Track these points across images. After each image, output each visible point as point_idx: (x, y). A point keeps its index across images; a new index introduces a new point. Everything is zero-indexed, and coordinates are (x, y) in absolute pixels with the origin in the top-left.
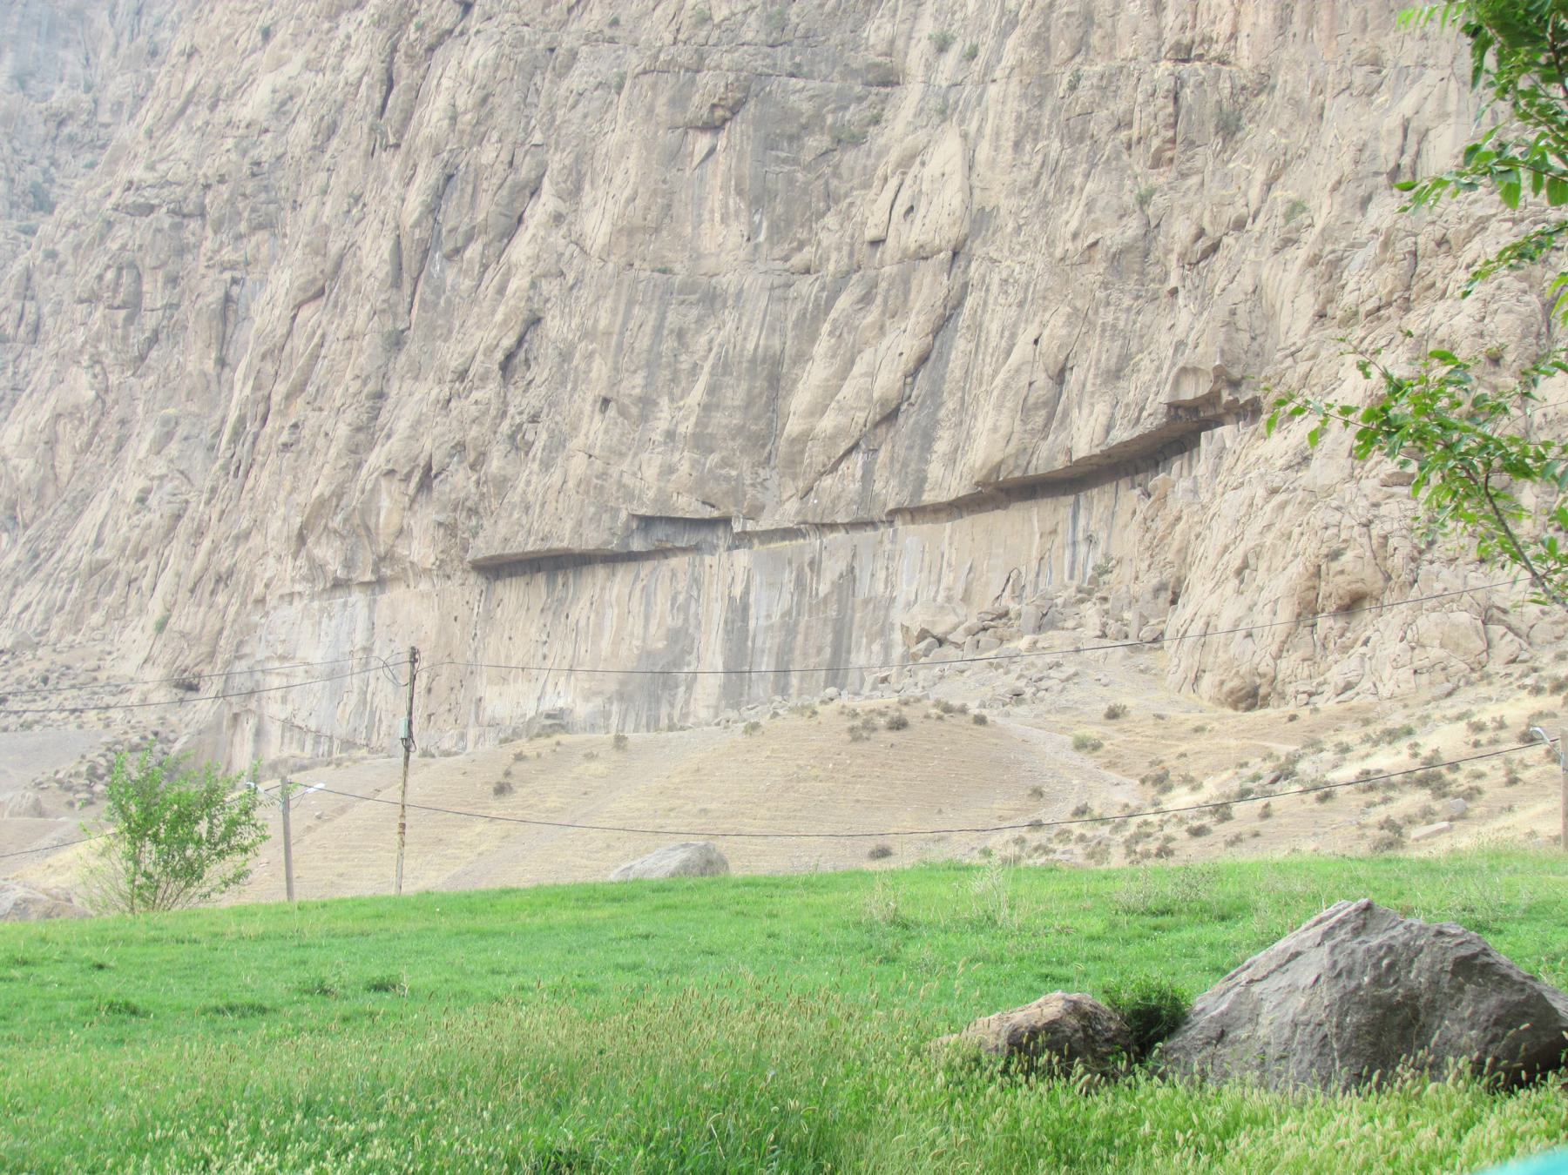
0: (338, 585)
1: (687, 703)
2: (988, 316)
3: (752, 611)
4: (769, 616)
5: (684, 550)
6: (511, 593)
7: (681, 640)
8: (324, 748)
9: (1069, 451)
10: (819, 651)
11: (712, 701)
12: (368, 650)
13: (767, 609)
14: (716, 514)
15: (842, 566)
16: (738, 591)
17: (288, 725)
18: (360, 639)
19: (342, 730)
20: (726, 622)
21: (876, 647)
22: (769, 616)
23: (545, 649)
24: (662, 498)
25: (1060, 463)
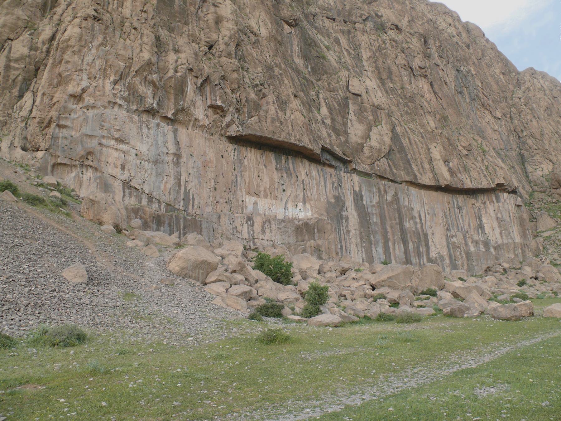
0: (150, 112)
1: (347, 226)
2: (412, 137)
3: (364, 198)
4: (371, 202)
5: (331, 166)
6: (251, 156)
7: (339, 202)
8: (155, 206)
9: (463, 184)
10: (395, 219)
11: (357, 227)
12: (178, 156)
13: (370, 199)
14: (347, 158)
15: (393, 193)
16: (357, 189)
17: (127, 185)
18: (172, 148)
19: (165, 198)
20: (354, 199)
21: (411, 221)
22: (371, 202)
23: (284, 187)
24: (331, 144)
25: (459, 186)
